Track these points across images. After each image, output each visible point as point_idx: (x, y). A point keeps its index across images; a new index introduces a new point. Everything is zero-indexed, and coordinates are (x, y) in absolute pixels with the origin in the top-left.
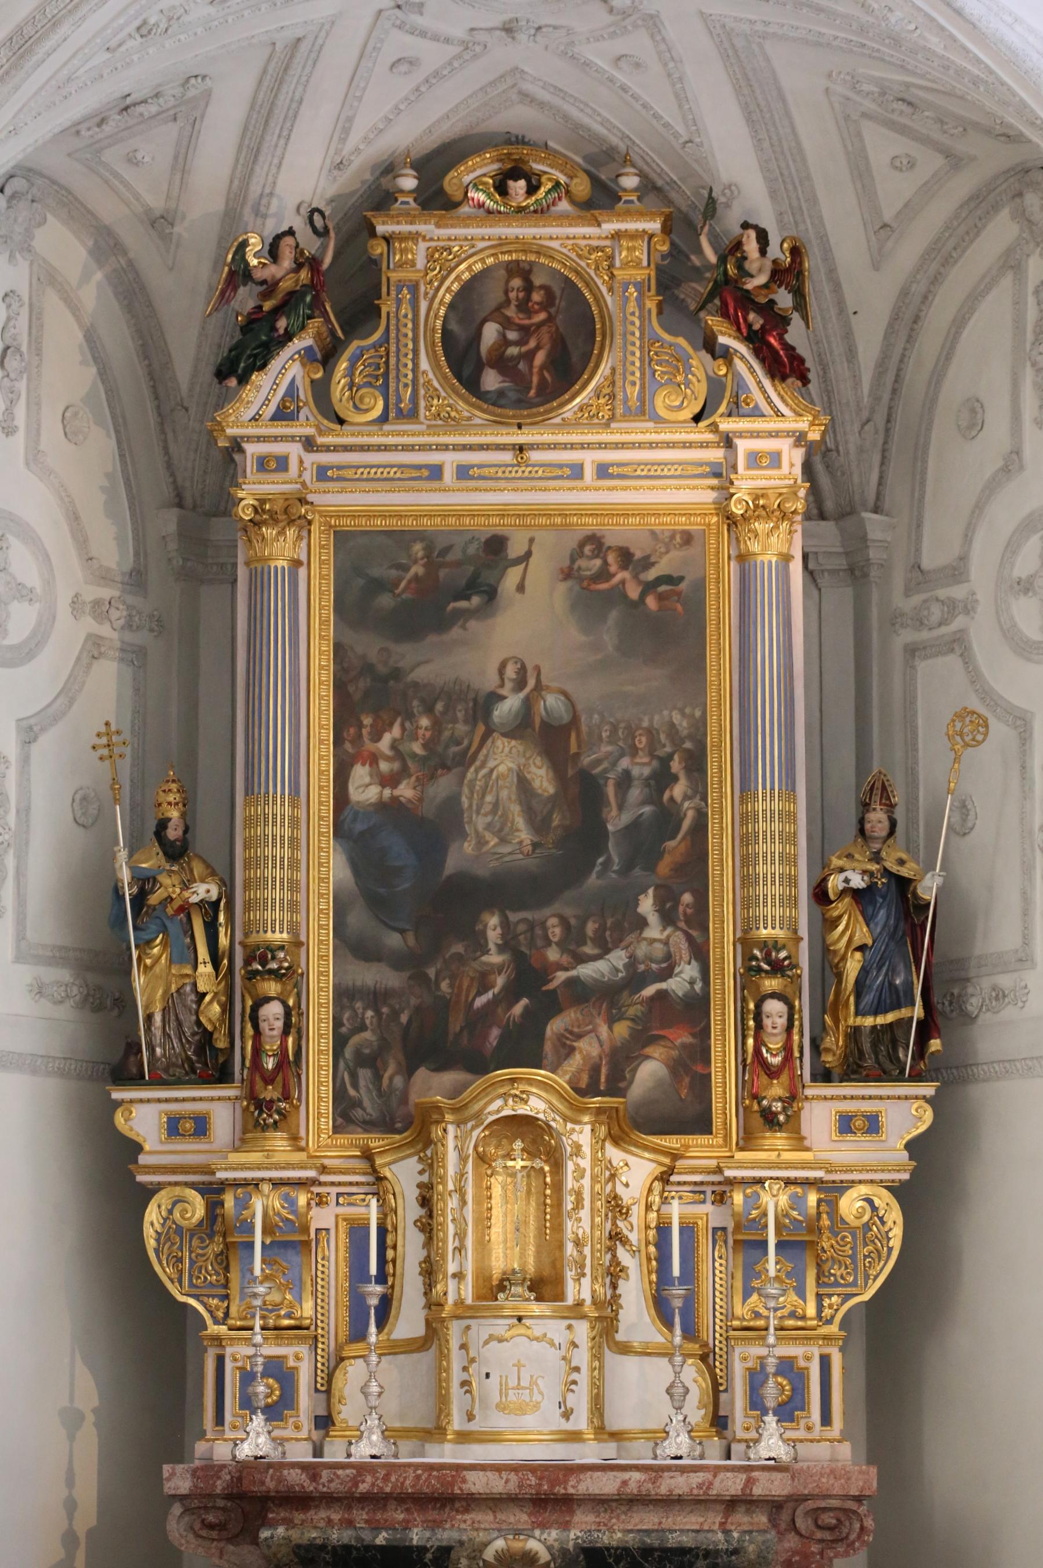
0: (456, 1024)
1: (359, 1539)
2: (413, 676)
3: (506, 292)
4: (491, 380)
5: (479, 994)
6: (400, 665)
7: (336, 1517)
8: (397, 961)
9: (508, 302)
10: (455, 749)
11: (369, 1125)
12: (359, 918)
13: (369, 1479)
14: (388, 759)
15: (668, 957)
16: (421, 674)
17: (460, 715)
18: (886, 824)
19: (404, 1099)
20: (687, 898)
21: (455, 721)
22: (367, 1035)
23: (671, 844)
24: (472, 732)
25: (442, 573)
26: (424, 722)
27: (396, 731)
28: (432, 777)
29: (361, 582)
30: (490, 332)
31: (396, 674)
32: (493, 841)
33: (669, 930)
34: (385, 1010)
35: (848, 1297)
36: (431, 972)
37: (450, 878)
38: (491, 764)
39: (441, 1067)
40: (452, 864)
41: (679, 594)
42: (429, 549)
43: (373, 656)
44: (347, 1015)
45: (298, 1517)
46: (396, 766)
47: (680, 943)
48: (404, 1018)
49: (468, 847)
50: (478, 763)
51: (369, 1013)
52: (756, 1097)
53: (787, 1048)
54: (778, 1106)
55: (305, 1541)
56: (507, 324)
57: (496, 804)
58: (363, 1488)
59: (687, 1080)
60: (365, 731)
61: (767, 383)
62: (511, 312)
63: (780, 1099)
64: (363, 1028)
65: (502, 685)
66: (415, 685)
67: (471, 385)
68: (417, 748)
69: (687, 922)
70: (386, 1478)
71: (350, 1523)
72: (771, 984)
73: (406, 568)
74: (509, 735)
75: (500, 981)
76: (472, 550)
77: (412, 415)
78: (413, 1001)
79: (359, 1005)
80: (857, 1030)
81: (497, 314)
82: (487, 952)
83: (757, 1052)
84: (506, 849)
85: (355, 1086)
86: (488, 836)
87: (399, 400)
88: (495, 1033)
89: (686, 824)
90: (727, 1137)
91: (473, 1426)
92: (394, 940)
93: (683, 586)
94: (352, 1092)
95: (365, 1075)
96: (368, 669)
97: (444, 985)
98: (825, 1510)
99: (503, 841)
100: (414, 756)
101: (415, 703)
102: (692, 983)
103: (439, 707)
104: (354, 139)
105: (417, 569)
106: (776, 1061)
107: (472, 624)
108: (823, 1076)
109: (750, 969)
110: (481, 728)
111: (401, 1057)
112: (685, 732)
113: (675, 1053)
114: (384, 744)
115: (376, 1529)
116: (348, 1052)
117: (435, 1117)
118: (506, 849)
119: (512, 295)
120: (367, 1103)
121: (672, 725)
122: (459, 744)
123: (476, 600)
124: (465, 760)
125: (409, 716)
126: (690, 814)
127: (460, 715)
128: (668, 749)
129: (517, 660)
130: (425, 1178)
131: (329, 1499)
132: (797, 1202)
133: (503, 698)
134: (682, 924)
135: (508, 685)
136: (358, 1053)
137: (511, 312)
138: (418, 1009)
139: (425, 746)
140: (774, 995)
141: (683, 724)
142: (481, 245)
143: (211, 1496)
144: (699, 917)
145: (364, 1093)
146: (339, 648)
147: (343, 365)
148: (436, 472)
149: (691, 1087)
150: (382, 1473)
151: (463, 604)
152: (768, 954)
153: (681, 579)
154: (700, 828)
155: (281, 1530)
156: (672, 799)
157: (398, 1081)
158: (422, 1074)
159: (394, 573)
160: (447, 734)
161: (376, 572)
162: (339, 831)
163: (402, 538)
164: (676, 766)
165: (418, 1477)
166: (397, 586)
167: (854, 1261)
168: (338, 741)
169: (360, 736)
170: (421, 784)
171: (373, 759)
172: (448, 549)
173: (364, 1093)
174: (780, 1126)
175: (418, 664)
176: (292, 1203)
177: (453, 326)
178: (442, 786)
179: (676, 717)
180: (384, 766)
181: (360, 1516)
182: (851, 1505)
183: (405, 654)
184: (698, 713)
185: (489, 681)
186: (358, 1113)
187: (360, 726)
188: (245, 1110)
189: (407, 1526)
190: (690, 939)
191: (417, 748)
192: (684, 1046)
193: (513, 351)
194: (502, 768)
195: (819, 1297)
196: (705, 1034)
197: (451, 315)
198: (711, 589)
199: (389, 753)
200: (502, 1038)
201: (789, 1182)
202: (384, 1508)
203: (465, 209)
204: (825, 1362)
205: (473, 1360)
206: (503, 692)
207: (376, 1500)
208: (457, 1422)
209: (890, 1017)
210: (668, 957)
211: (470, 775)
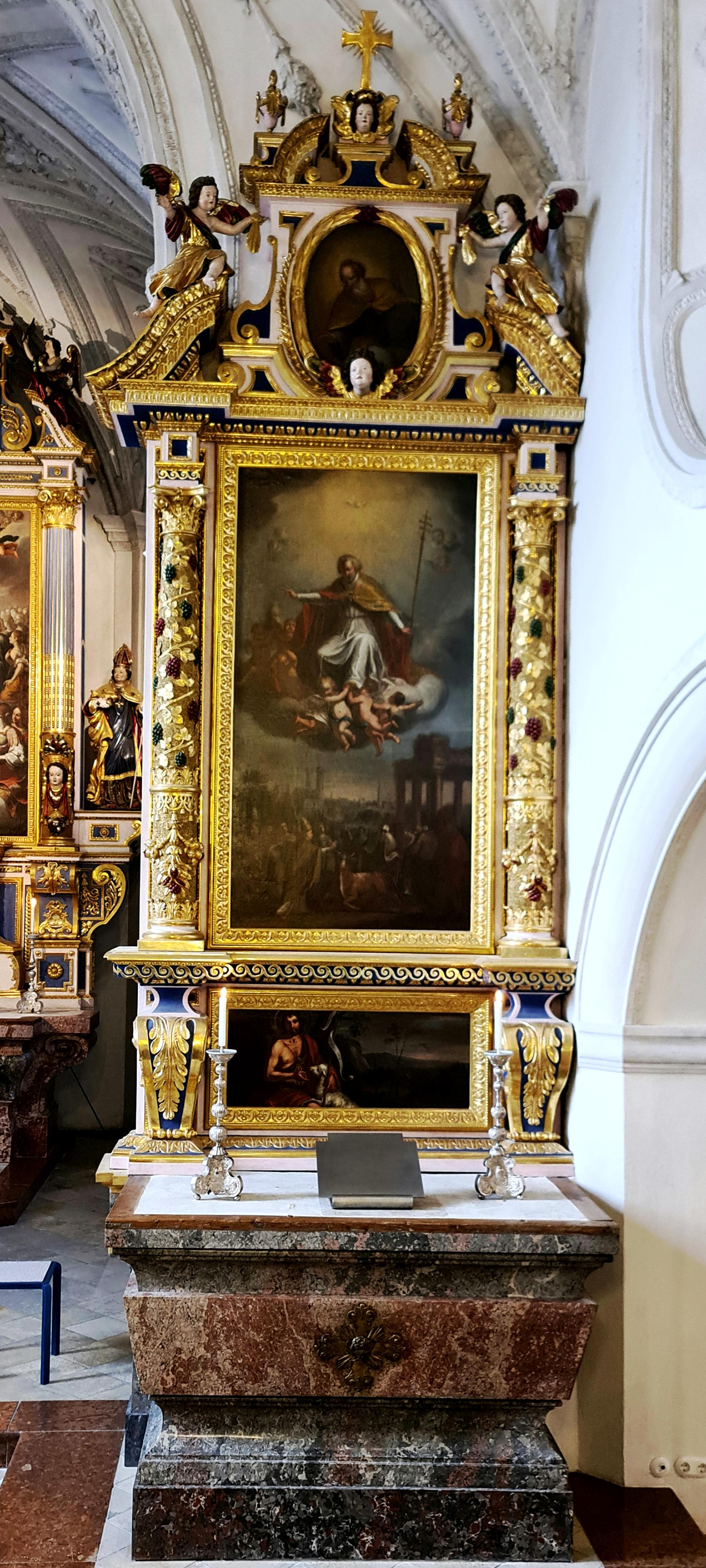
15: (6, 742)
18: (125, 673)
20: (17, 711)
23: (9, 682)
33: (7, 727)
35: (95, 922)
41: (16, 546)
47: (12, 735)
52: (47, 818)
53: (64, 792)
54: (56, 822)
59: (14, 808)
61: (58, 429)
63: (57, 819)
69: (17, 724)
72: (56, 758)
80: (106, 782)
83: (47, 793)
89: (17, 671)
90: (35, 837)
93: (18, 542)
98: (61, 1041)
102: (19, 756)
106: (56, 799)
108: (87, 805)
109: (45, 749)
112: (17, 622)
113: (8, 793)
121: (11, 618)
126: (20, 666)
128: (8, 630)
132: (64, 874)
134: (14, 725)
140: (56, 764)
141: (17, 618)
144: (23, 722)
149: (17, 810)
152: (53, 742)
153: (17, 538)
154: (25, 674)
156: (10, 657)
164: (12, 640)
167: (100, 904)
174: (59, 834)
179: (13, 614)
182: (76, 1038)
184: (25, 612)
190: (18, 732)
192: (13, 789)
195: (80, 923)
196: (24, 784)
198: (33, 544)
201: (60, 863)
204: (82, 957)
209: (122, 777)
210: (6, 742)
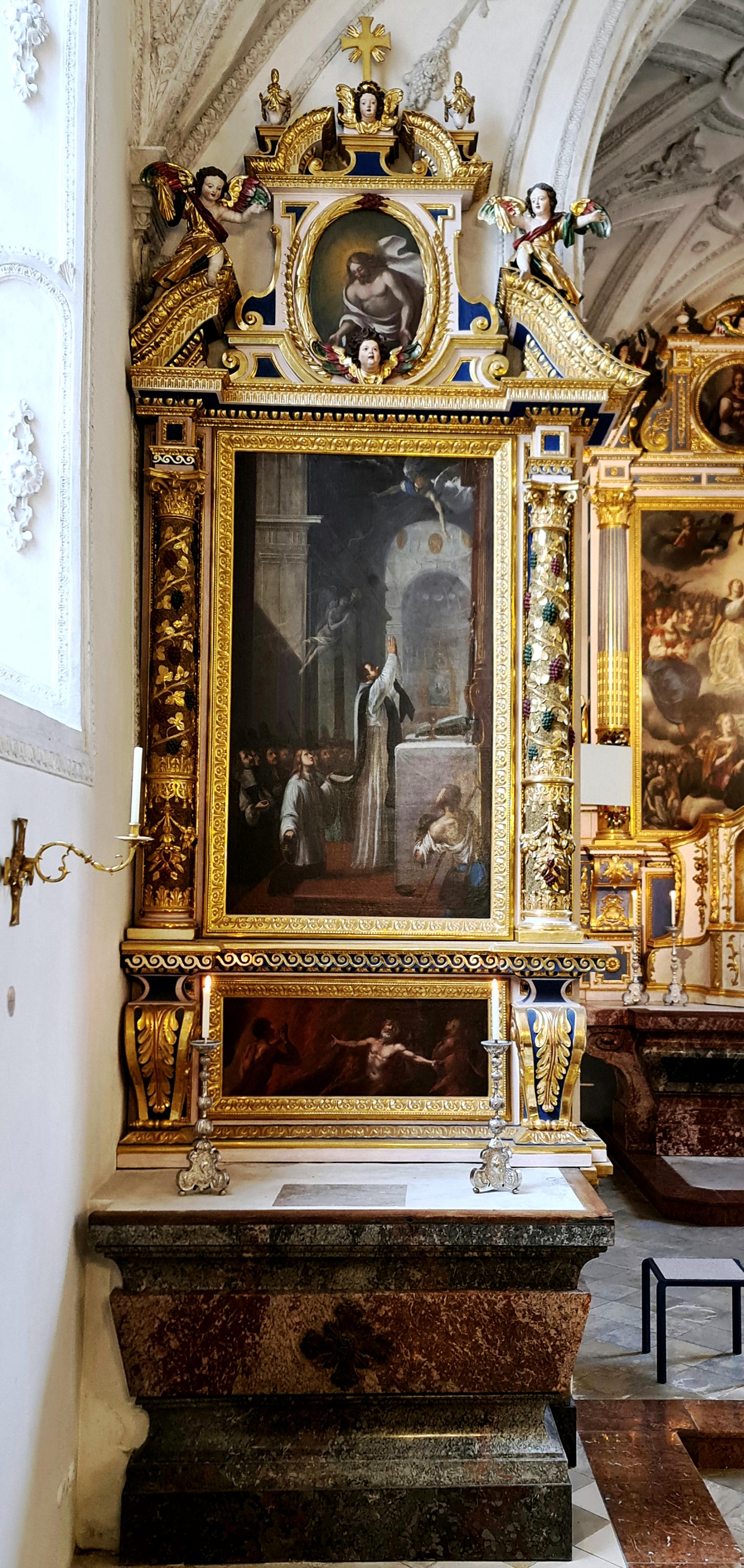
0: (706, 773)
1: (698, 1055)
2: (683, 589)
3: (733, 382)
4: (725, 430)
5: (718, 758)
6: (679, 582)
7: (683, 1042)
8: (675, 740)
9: (734, 387)
10: (705, 628)
11: (661, 826)
12: (655, 717)
13: (705, 1023)
14: (671, 633)
16: (688, 588)
17: (708, 610)
19: (679, 812)
21: (705, 613)
22: (659, 778)
24: (714, 620)
25: (699, 534)
26: (689, 613)
27: (674, 618)
28: (693, 643)
29: (655, 538)
30: (725, 403)
31: (674, 588)
32: (726, 677)
34: (669, 765)
36: (693, 746)
37: (703, 696)
38: (724, 636)
39: (698, 796)
40: (704, 689)
42: (692, 521)
43: (662, 579)
44: (649, 768)
45: (663, 1042)
46: (674, 637)
48: (679, 770)
49: (713, 680)
50: (718, 635)
51: (661, 767)
55: (668, 1055)
56: (733, 399)
57: (727, 657)
58: (701, 1027)
60: (658, 618)
62: (736, 392)
64: (657, 775)
65: (730, 594)
66: (685, 594)
67: (714, 433)
68: (685, 627)
70: (714, 1023)
71: (690, 1046)
73: (680, 531)
74: (734, 620)
75: (729, 751)
76: (715, 521)
77: (686, 447)
78: (684, 761)
79: (655, 763)
81: (729, 393)
82: (722, 735)
84: (731, 682)
85: (654, 805)
86: (723, 674)
87: (677, 439)
88: (727, 778)
91: (735, 988)
92: (673, 729)
94: (652, 808)
95: (658, 799)
96: (660, 585)
97: (700, 753)
99: (731, 677)
100: (684, 632)
101: (684, 603)
103: (697, 605)
104: (658, 295)
105: (685, 532)
107: (715, 561)
110: (719, 618)
111: (678, 790)
114: (668, 625)
115: (708, 1050)
116: (650, 787)
117: (711, 823)
118: (731, 682)
119: (737, 383)
120: (659, 813)
122: (708, 625)
123: (717, 549)
124: (709, 634)
125: (682, 610)
127: (708, 610)
129: (739, 581)
130: (699, 855)
131: (679, 1034)
133: (730, 601)
135: (734, 594)
136: (655, 787)
137: (736, 392)
138: (686, 765)
139: (689, 626)
142: (722, 355)
143: (607, 1026)
145: (657, 808)
146: (644, 573)
147: (648, 420)
148: (698, 479)
150: (711, 1020)
151: (709, 551)
155: (655, 1050)
157: (676, 803)
158: (688, 798)
159: (673, 533)
160: (701, 620)
161: (663, 533)
162: (644, 673)
163: (676, 516)
165: (732, 1023)
166: (674, 540)
168: (644, 623)
169: (655, 620)
170: (687, 647)
171: (662, 633)
172: (701, 521)
173: (657, 808)
175: (686, 583)
176: (631, 868)
177: (706, 400)
178: (699, 648)
180: (668, 637)
181: (697, 1042)
183: (679, 577)
185: (723, 592)
186: (655, 819)
187: (655, 615)
188: (599, 817)
189: (722, 1048)
191: (685, 627)
193: (737, 413)
194: (730, 639)
197: (705, 394)
199: (671, 630)
200: (730, 781)
202: (710, 1038)
203: (715, 334)
205: (735, 954)
206: (731, 598)
207: (707, 1034)
208: (726, 985)
211: (714, 641)
